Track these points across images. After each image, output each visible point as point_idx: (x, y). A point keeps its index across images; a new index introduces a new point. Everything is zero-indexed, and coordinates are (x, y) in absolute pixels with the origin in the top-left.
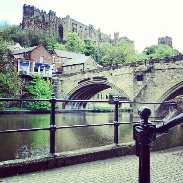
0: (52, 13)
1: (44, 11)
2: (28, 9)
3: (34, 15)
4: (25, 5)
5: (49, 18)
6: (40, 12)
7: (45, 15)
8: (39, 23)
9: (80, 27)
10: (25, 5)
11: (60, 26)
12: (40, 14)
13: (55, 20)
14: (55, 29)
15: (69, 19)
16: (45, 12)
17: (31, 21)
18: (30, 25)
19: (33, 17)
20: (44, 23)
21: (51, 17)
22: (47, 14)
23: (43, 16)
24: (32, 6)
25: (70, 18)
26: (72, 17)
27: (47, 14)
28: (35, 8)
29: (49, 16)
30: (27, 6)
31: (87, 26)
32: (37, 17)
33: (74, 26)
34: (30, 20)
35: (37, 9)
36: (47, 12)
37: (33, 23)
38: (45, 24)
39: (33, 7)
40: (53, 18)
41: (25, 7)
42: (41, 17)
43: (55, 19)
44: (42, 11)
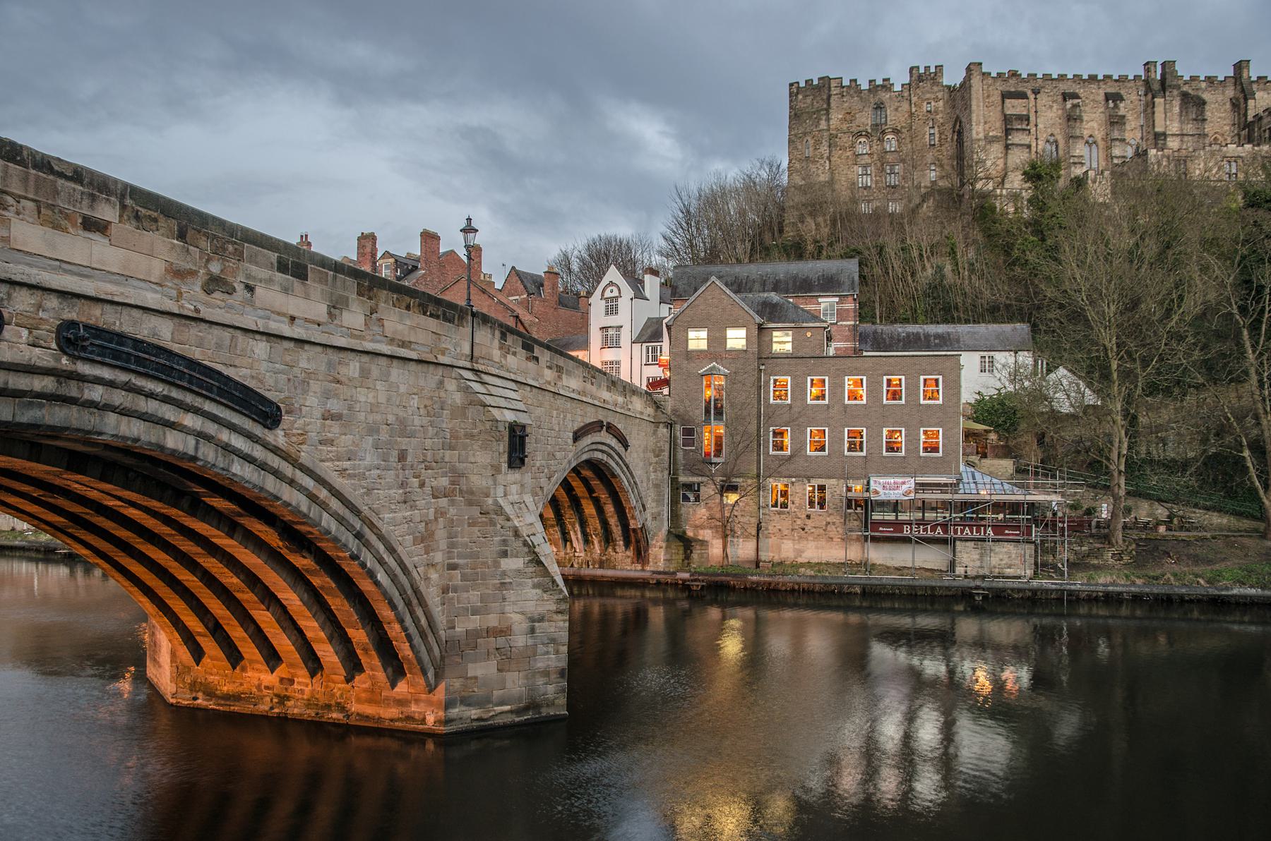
0: (920, 78)
1: (879, 82)
2: (805, 96)
3: (828, 114)
4: (791, 85)
5: (905, 106)
6: (861, 91)
7: (885, 96)
8: (862, 140)
9: (1060, 98)
10: (791, 85)
11: (957, 127)
12: (861, 98)
13: (941, 103)
14: (941, 145)
15: (976, 81)
16: (887, 86)
17: (818, 143)
18: (815, 162)
19: (823, 125)
20: (883, 132)
21: (914, 99)
22: (897, 88)
23: (879, 107)
24: (820, 79)
25: (986, 75)
26: (992, 68)
27: (897, 88)
28: (833, 84)
29: (906, 94)
30: (802, 84)
31: (1123, 79)
32: (849, 116)
33: (1014, 107)
34: (811, 142)
35: (846, 83)
36: (900, 79)
37: (824, 149)
38: (890, 137)
39: (826, 81)
40: (928, 96)
41: (795, 91)
42: (869, 111)
43: (936, 99)
44: (870, 81)
